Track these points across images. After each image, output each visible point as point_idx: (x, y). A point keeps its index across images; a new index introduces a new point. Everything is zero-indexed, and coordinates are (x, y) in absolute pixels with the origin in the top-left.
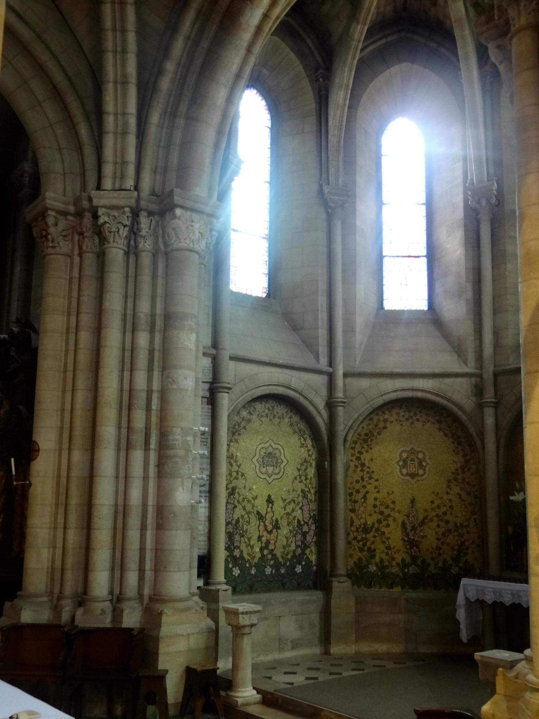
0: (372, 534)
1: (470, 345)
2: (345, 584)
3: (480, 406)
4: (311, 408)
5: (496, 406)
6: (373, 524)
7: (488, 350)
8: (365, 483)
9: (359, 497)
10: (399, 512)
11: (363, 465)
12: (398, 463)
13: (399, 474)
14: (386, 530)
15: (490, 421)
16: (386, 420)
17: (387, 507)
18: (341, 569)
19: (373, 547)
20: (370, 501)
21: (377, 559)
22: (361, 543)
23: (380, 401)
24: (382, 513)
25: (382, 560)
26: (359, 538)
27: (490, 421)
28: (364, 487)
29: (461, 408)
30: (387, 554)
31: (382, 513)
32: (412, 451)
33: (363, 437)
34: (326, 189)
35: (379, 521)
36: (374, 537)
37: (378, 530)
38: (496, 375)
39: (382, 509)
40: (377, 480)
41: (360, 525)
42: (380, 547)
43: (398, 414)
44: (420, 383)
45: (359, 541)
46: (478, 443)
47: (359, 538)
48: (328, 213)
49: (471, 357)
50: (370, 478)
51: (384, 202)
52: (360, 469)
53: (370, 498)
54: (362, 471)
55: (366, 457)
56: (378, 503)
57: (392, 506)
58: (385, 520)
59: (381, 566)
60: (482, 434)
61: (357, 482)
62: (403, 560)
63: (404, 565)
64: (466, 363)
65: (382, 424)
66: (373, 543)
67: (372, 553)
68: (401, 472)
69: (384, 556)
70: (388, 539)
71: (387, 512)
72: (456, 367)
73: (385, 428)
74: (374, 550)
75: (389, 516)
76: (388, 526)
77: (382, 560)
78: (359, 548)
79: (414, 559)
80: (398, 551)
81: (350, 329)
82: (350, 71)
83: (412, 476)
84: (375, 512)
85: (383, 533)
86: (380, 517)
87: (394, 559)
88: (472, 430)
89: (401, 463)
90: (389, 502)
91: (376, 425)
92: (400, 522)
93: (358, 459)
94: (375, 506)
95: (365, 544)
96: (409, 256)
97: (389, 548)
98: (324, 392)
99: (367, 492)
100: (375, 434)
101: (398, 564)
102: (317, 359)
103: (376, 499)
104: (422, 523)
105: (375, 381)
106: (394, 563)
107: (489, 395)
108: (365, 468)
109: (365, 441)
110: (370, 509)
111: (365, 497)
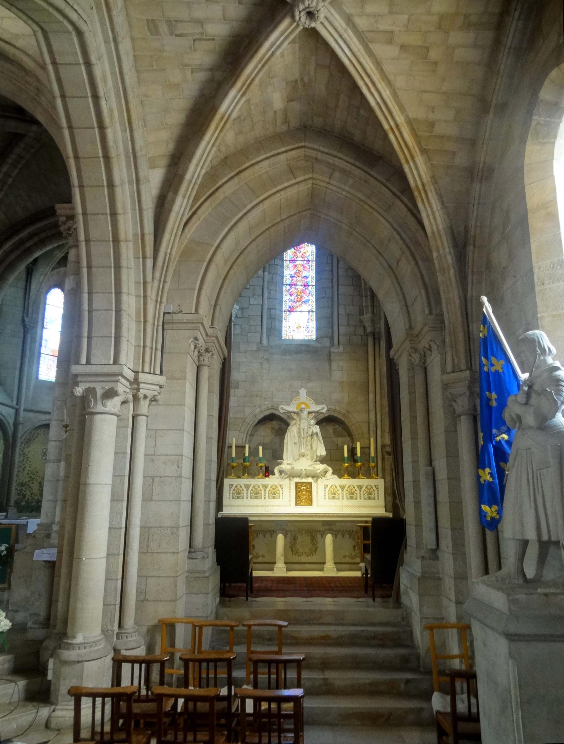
0: (25, 487)
2: (13, 510)
4: (7, 425)
6: (26, 482)
8: (24, 463)
9: (22, 468)
10: (39, 477)
11: (24, 454)
12: (41, 454)
13: (41, 459)
14: (32, 485)
16: (38, 434)
17: (34, 474)
18: (12, 503)
19: (25, 493)
20: (26, 471)
21: (26, 499)
22: (19, 492)
23: (39, 424)
24: (31, 477)
25: (28, 499)
26: (18, 489)
28: (24, 464)
30: (31, 496)
31: (31, 477)
33: (26, 441)
34: (26, 319)
35: (29, 481)
36: (26, 488)
37: (28, 485)
39: (31, 475)
40: (30, 462)
41: (20, 483)
42: (28, 493)
43: (44, 431)
45: (18, 490)
47: (18, 489)
48: (24, 330)
50: (27, 460)
51: (45, 327)
52: (22, 456)
53: (26, 469)
54: (24, 457)
55: (26, 451)
56: (29, 472)
57: (36, 474)
58: (32, 480)
59: (28, 502)
61: (21, 462)
62: (38, 499)
65: (36, 435)
66: (25, 491)
67: (24, 496)
68: (42, 458)
69: (30, 498)
70: (32, 489)
71: (33, 477)
73: (37, 437)
74: (26, 495)
75: (34, 478)
76: (33, 483)
77: (28, 499)
78: (18, 494)
80: (36, 495)
81: (28, 388)
82: (49, 269)
84: (28, 477)
85: (31, 487)
86: (30, 479)
87: (34, 499)
89: (42, 454)
90: (35, 472)
91: (33, 435)
92: (39, 481)
93: (23, 451)
94: (28, 474)
95: (21, 492)
96: (54, 356)
97: (32, 494)
98: (13, 417)
99: (25, 467)
100: (32, 439)
101: (36, 501)
102: (12, 401)
103: (29, 471)
105: (37, 414)
106: (34, 501)
108: (25, 456)
109: (27, 442)
110: (25, 475)
111: (24, 469)
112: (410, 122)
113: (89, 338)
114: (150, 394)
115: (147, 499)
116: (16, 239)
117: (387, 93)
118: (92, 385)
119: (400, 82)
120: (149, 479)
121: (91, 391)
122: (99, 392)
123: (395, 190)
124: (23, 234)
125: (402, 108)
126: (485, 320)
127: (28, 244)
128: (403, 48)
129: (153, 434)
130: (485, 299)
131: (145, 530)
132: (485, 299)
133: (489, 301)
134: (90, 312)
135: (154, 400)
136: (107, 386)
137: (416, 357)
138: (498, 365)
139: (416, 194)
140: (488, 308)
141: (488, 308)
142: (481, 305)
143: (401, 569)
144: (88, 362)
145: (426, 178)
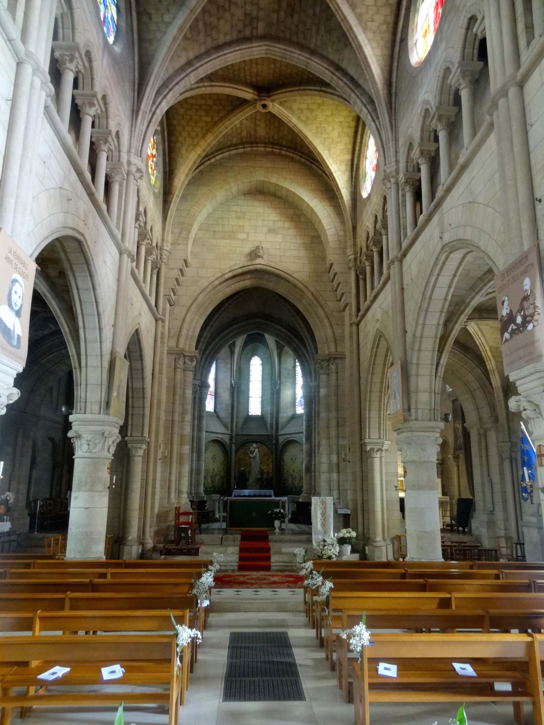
1: (229, 426)
3: (231, 444)
5: (235, 444)
7: (234, 428)
15: (234, 447)
27: (234, 447)
29: (226, 443)
32: (214, 455)
38: (236, 435)
44: (220, 436)
46: (229, 452)
49: (230, 429)
60: (231, 452)
63: (211, 488)
64: (228, 430)
72: (227, 432)
79: (213, 486)
83: (214, 462)
88: (229, 450)
104: (215, 476)
107: (234, 441)
112: (490, 348)
113: (369, 428)
114: (386, 448)
115: (387, 490)
116: (222, 335)
117: (483, 340)
118: (373, 447)
119: (487, 335)
120: (387, 481)
121: (372, 449)
122: (375, 449)
123: (477, 364)
124: (225, 333)
125: (487, 343)
126: (522, 431)
127: (226, 338)
128: (491, 327)
129: (387, 464)
130: (522, 423)
131: (387, 501)
132: (522, 423)
133: (524, 424)
134: (369, 418)
135: (387, 450)
136: (378, 447)
137: (482, 431)
138: (527, 448)
139: (490, 372)
140: (523, 427)
141: (523, 427)
142: (521, 425)
143: (472, 520)
144: (369, 438)
145: (494, 367)
